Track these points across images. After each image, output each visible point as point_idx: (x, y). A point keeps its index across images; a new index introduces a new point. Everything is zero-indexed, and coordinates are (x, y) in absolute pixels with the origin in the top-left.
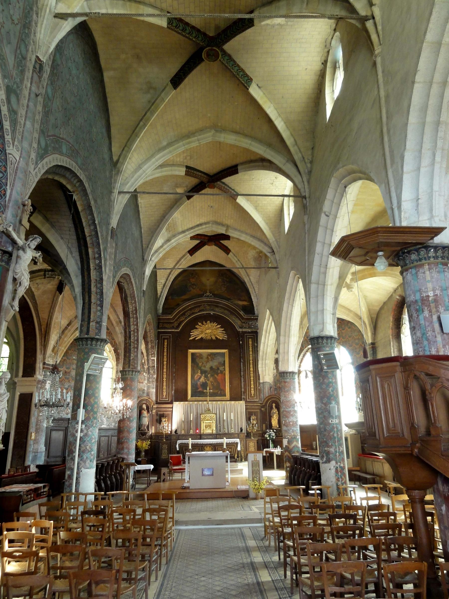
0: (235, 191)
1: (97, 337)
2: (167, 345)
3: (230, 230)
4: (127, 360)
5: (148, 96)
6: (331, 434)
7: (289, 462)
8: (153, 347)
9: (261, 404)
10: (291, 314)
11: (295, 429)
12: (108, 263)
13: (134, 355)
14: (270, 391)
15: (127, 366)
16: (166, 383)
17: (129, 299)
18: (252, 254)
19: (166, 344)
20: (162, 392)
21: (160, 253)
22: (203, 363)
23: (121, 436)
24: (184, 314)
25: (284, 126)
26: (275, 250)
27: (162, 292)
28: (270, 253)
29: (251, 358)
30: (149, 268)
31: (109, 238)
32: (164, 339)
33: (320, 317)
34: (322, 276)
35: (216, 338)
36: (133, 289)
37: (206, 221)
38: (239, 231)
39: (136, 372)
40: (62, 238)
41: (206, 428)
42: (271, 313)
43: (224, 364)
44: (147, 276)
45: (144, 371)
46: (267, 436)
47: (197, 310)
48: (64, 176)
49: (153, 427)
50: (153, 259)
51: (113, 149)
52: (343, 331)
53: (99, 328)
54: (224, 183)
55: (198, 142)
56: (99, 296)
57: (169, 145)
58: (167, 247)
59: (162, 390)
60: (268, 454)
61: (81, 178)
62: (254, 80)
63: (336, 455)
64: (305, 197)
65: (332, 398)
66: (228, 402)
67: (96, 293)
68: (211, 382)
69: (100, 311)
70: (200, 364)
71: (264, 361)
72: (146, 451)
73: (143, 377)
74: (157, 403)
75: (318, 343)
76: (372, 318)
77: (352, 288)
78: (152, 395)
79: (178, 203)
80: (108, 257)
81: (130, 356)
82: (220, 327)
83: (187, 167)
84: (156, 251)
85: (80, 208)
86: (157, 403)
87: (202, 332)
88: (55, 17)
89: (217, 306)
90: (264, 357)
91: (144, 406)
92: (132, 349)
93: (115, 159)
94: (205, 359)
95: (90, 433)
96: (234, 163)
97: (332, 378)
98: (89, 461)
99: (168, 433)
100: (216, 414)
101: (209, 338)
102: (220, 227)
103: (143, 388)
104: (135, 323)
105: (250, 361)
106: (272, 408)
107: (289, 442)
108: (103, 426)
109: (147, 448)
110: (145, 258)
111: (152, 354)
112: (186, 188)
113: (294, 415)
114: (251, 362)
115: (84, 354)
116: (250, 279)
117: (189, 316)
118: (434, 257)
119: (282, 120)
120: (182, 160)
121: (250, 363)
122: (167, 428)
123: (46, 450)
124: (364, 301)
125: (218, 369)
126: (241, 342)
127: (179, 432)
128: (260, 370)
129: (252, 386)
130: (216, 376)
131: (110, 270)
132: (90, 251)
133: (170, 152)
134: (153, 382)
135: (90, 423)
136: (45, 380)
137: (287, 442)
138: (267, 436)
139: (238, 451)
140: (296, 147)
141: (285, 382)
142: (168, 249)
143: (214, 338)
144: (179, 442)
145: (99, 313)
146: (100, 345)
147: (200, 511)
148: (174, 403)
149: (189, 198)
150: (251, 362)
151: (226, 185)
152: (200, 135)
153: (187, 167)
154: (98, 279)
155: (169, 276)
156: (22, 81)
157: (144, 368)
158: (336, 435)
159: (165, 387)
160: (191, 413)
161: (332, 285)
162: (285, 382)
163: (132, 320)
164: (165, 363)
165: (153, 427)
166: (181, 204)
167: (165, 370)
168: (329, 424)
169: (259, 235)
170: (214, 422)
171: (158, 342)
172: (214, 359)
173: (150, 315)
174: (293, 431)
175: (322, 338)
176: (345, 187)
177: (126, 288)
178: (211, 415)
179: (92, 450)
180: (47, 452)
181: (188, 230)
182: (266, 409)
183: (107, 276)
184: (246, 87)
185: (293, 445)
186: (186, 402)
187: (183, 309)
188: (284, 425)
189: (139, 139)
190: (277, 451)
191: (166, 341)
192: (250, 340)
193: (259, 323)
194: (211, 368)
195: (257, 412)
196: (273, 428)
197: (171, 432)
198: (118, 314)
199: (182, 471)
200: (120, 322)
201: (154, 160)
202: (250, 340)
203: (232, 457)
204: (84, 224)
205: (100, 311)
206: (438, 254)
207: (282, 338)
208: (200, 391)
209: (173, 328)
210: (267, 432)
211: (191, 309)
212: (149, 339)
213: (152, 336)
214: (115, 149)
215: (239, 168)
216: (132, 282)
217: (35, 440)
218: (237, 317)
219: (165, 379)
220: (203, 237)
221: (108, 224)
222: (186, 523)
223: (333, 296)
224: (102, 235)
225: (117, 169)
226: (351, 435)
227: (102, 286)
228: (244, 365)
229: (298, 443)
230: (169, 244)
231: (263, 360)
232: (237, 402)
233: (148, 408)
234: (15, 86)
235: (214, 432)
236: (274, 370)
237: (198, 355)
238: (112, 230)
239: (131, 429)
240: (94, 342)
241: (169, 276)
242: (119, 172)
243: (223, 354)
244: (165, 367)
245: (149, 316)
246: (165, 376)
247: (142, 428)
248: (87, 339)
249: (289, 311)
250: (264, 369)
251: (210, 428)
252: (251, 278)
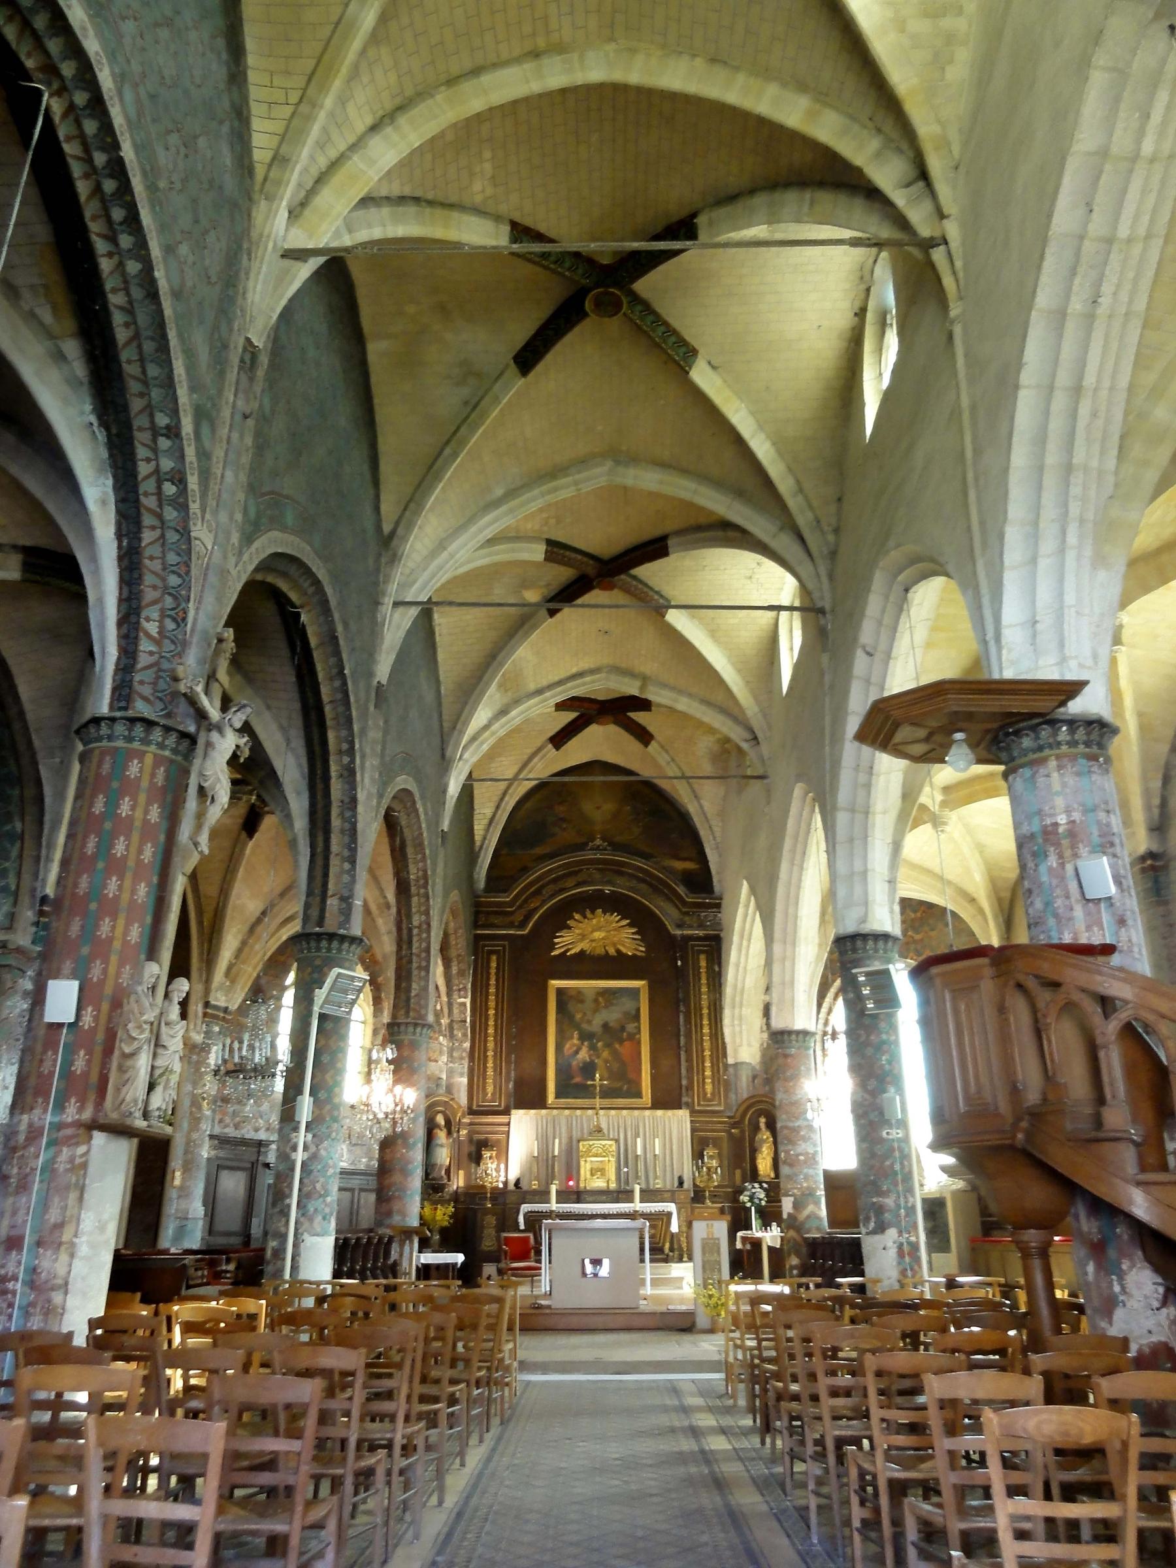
0: (662, 596)
1: (342, 932)
2: (498, 968)
3: (651, 688)
4: (403, 997)
5: (465, 392)
6: (888, 1163)
7: (798, 1255)
8: (461, 973)
9: (729, 1117)
10: (799, 887)
11: (811, 1172)
12: (368, 764)
14: (754, 1087)
15: (402, 1012)
16: (494, 1063)
17: (410, 851)
18: (705, 745)
19: (494, 965)
20: (485, 1083)
21: (482, 743)
22: (585, 1014)
23: (387, 1182)
24: (538, 892)
25: (772, 451)
26: (760, 735)
27: (484, 838)
28: (746, 741)
29: (705, 1003)
30: (457, 778)
31: (372, 708)
32: (491, 952)
33: (858, 890)
34: (861, 793)
35: (618, 951)
36: (420, 827)
37: (592, 666)
38: (673, 688)
39: (424, 1026)
40: (269, 707)
41: (592, 1175)
42: (753, 890)
43: (637, 1017)
44: (452, 797)
45: (440, 1032)
46: (746, 1199)
47: (570, 882)
48: (284, 575)
49: (461, 1173)
50: (466, 756)
51: (384, 507)
52: (933, 934)
53: (346, 912)
54: (635, 578)
55: (573, 488)
56: (347, 839)
57: (511, 494)
58: (501, 728)
59: (485, 1079)
60: (748, 1247)
61: (320, 577)
62: (702, 352)
63: (898, 1216)
64: (821, 611)
65: (888, 1079)
66: (647, 1113)
67: (342, 831)
68: (606, 1061)
69: (348, 872)
70: (578, 1016)
71: (737, 1011)
74: (471, 1112)
75: (854, 950)
76: (1000, 900)
77: (945, 824)
78: (459, 1091)
79: (526, 627)
80: (368, 751)
81: (409, 990)
82: (628, 925)
83: (550, 543)
84: (474, 739)
85: (313, 641)
86: (471, 1112)
87: (583, 937)
88: (283, 256)
89: (621, 873)
90: (737, 999)
91: (440, 1120)
92: (415, 972)
93: (387, 528)
94: (589, 1004)
95: (323, 1152)
96: (657, 532)
97: (887, 1033)
98: (320, 1218)
99: (497, 1188)
100: (617, 1141)
101: (600, 951)
102: (626, 680)
104: (423, 909)
105: (701, 1009)
106: (757, 1129)
107: (797, 1205)
109: (446, 1224)
110: (448, 753)
111: (459, 990)
112: (545, 591)
113: (810, 1138)
114: (705, 1011)
115: (313, 972)
116: (701, 807)
117: (552, 896)
118: (1068, 743)
119: (768, 437)
120: (537, 527)
121: (701, 1015)
122: (494, 1174)
123: (206, 1215)
124: (977, 855)
125: (623, 1029)
126: (679, 963)
127: (524, 1185)
128: (727, 1031)
129: (708, 1073)
130: (617, 1046)
131: (373, 780)
132: (331, 736)
133: (511, 511)
134: (462, 1058)
135: (324, 1130)
136: (208, 1045)
137: (791, 1205)
138: (746, 1199)
139: (672, 1235)
140: (800, 498)
141: (786, 1056)
142: (502, 733)
143: (612, 951)
144: (525, 1208)
145: (346, 878)
146: (348, 952)
147: (575, 1347)
148: (513, 1112)
149: (552, 613)
150: (705, 1011)
151: (641, 581)
152: (579, 472)
153: (550, 543)
154: (347, 800)
155: (502, 799)
156: (220, 391)
158: (897, 1167)
159: (490, 1072)
160: (554, 1138)
161: (885, 813)
162: (786, 1056)
163: (415, 900)
164: (492, 1012)
165: (461, 1173)
166: (535, 627)
167: (491, 1031)
168: (882, 1141)
169: (719, 697)
170: (613, 1160)
171: (476, 961)
172: (612, 1004)
173: (456, 892)
174: (806, 1178)
175: (864, 937)
176: (907, 590)
177: (403, 823)
178: (604, 1142)
179: (327, 1194)
180: (208, 1219)
181: (551, 687)
182: (743, 1132)
183: (365, 792)
184: (682, 368)
185: (806, 1213)
186: (544, 1112)
188: (785, 1162)
189: (441, 485)
190: (771, 1236)
191: (494, 958)
192: (703, 957)
193: (724, 916)
194: (605, 1026)
195: (720, 1138)
196: (760, 1178)
197: (506, 1183)
198: (384, 885)
199: (532, 1274)
200: (388, 906)
201: (473, 529)
202: (703, 957)
203: (656, 1250)
204: (321, 676)
205: (348, 872)
206: (1077, 737)
207: (777, 948)
208: (577, 1085)
209: (511, 925)
210: (745, 1189)
211: (555, 881)
212: (453, 953)
213: (460, 944)
214: (389, 508)
215: (671, 542)
216: (416, 811)
217: (182, 1188)
218: (668, 899)
219: (490, 1053)
220: (586, 705)
221: (370, 674)
222: (544, 1368)
223: (889, 840)
224: (357, 701)
225: (391, 552)
226: (955, 1193)
227: (355, 816)
228: (688, 1021)
229: (820, 1208)
230: (504, 720)
231: (734, 1007)
232: (670, 1113)
233: (448, 1123)
234: (209, 405)
235: (613, 1186)
236: (762, 1032)
237: (573, 993)
238: (378, 688)
239: (410, 1167)
240: (335, 944)
241: (502, 799)
242: (394, 559)
243: (635, 993)
244: (491, 1022)
245: (455, 896)
246: (491, 1045)
247: (434, 1175)
248: (319, 936)
249: (794, 881)
250: (737, 1029)
251: (603, 1174)
252: (706, 805)
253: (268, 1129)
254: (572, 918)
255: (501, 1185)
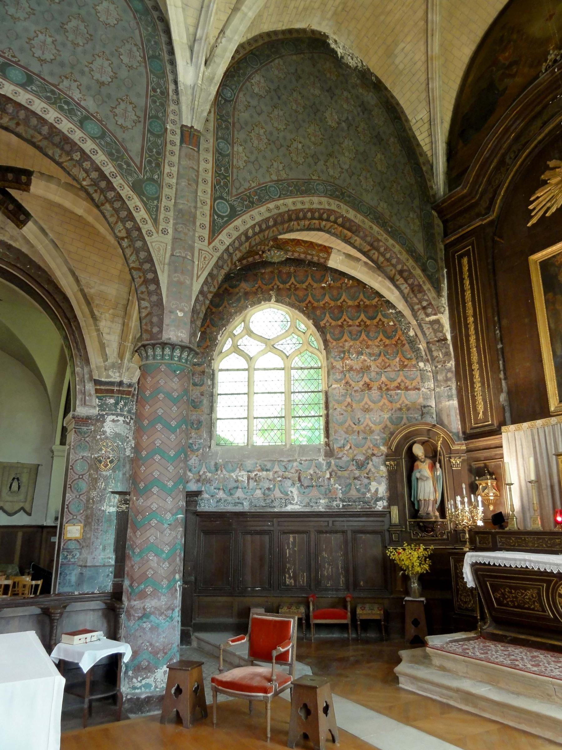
13: (150, 302)
24: (502, 162)
32: (461, 257)
39: (154, 345)
45: (419, 358)
72: (422, 578)
73: (414, 373)
78: (448, 416)
86: (468, 437)
91: (418, 450)
103: (421, 400)
108: (289, 508)
111: (424, 308)
134: (447, 380)
136: (103, 416)
157: (419, 349)
164: (471, 320)
187: (493, 152)
191: (465, 261)
239: (140, 517)
253: (198, 481)
254: (548, 168)
255: (480, 523)
